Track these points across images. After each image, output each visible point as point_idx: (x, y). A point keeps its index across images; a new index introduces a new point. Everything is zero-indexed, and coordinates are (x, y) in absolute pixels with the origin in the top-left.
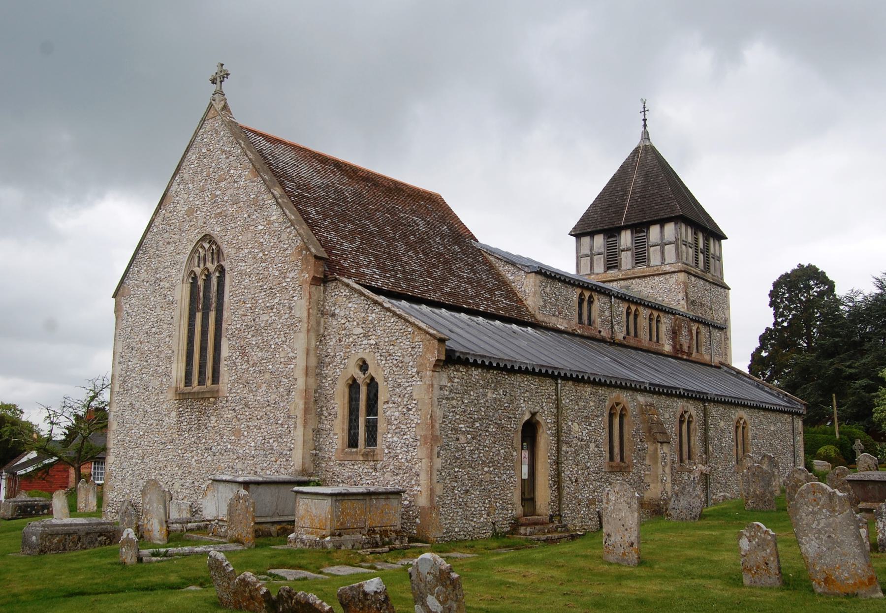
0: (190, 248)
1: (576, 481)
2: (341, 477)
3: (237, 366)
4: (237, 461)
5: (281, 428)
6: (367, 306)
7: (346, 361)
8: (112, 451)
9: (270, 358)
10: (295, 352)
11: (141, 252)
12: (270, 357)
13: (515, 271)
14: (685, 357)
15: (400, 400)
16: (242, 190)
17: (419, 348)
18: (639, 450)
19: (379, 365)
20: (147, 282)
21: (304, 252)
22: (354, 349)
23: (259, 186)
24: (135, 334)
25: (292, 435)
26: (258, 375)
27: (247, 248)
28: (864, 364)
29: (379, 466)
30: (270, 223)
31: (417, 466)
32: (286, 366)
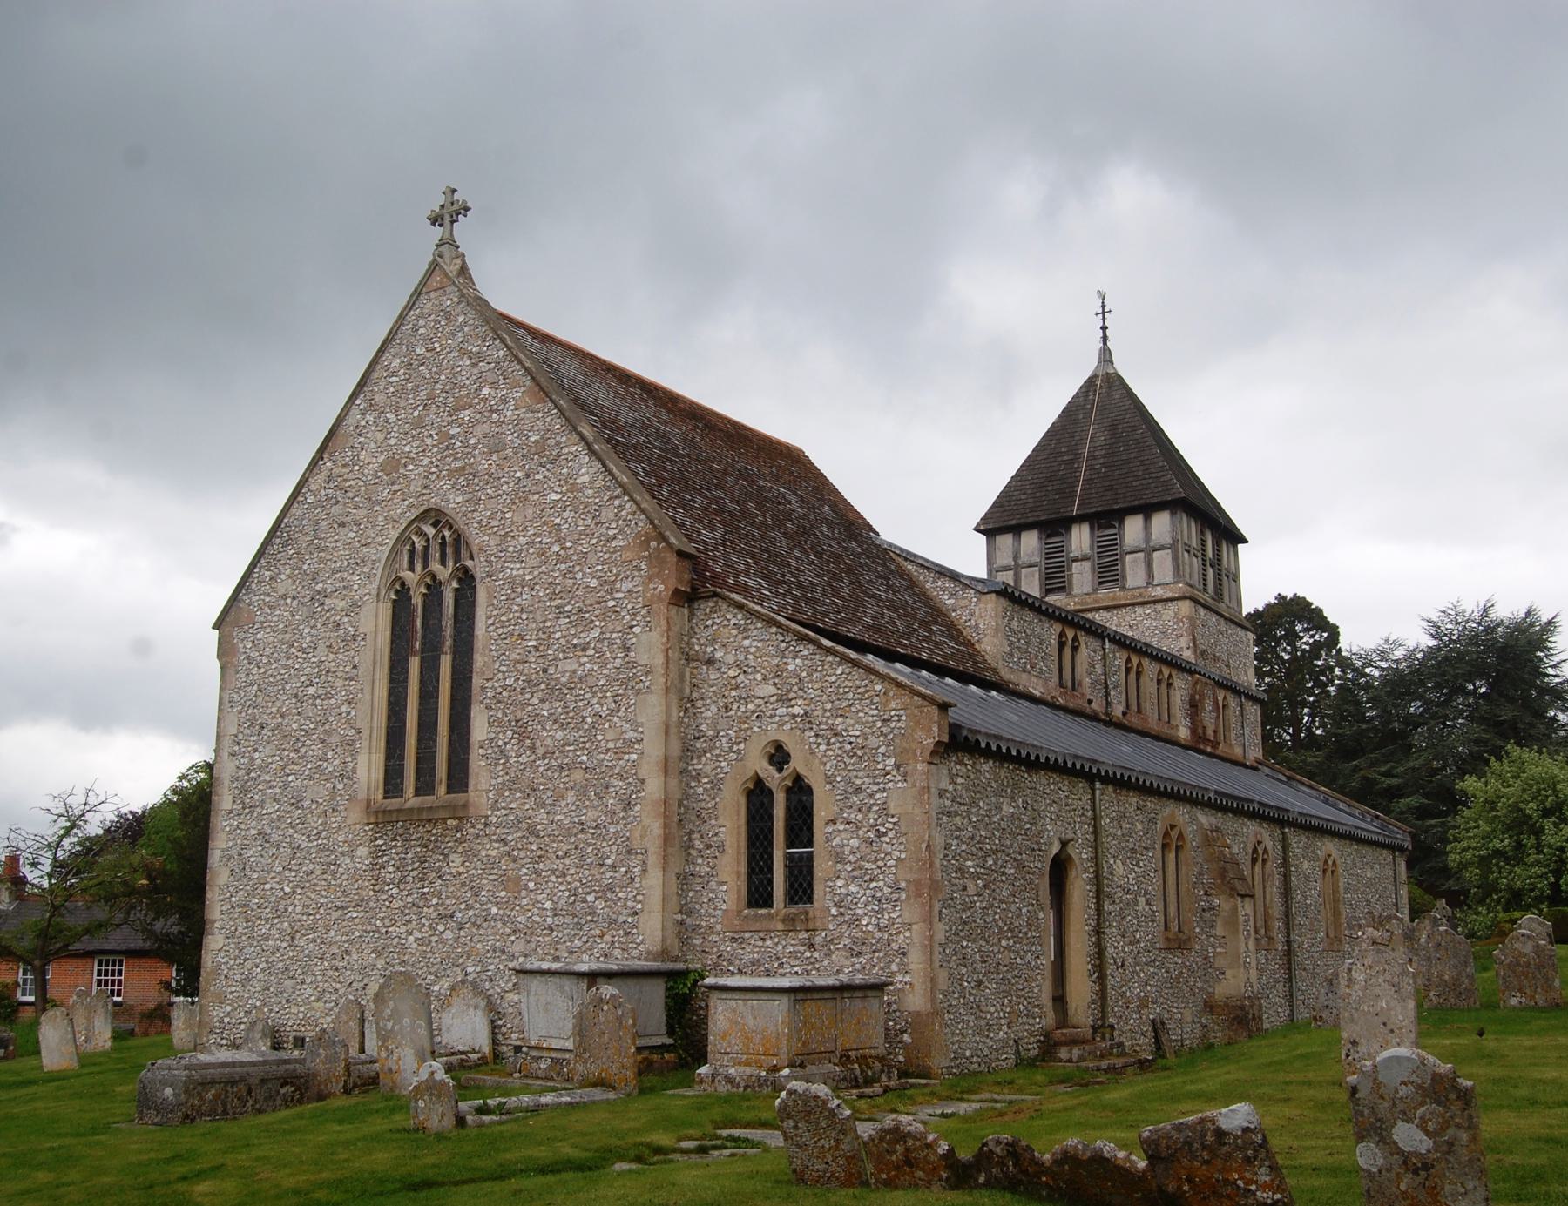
1: (1123, 965)
2: (737, 962)
3: (507, 758)
4: (513, 938)
5: (612, 874)
6: (784, 645)
7: (742, 746)
8: (217, 925)
9: (584, 742)
10: (640, 729)
11: (278, 541)
12: (582, 740)
13: (957, 589)
14: (1209, 749)
15: (860, 817)
16: (510, 427)
17: (899, 721)
18: (1204, 910)
19: (812, 753)
20: (294, 598)
21: (653, 544)
22: (759, 724)
23: (548, 419)
24: (267, 698)
25: (637, 885)
26: (556, 775)
27: (524, 536)
28: (1413, 769)
29: (818, 940)
30: (574, 488)
31: (902, 936)
32: (621, 755)
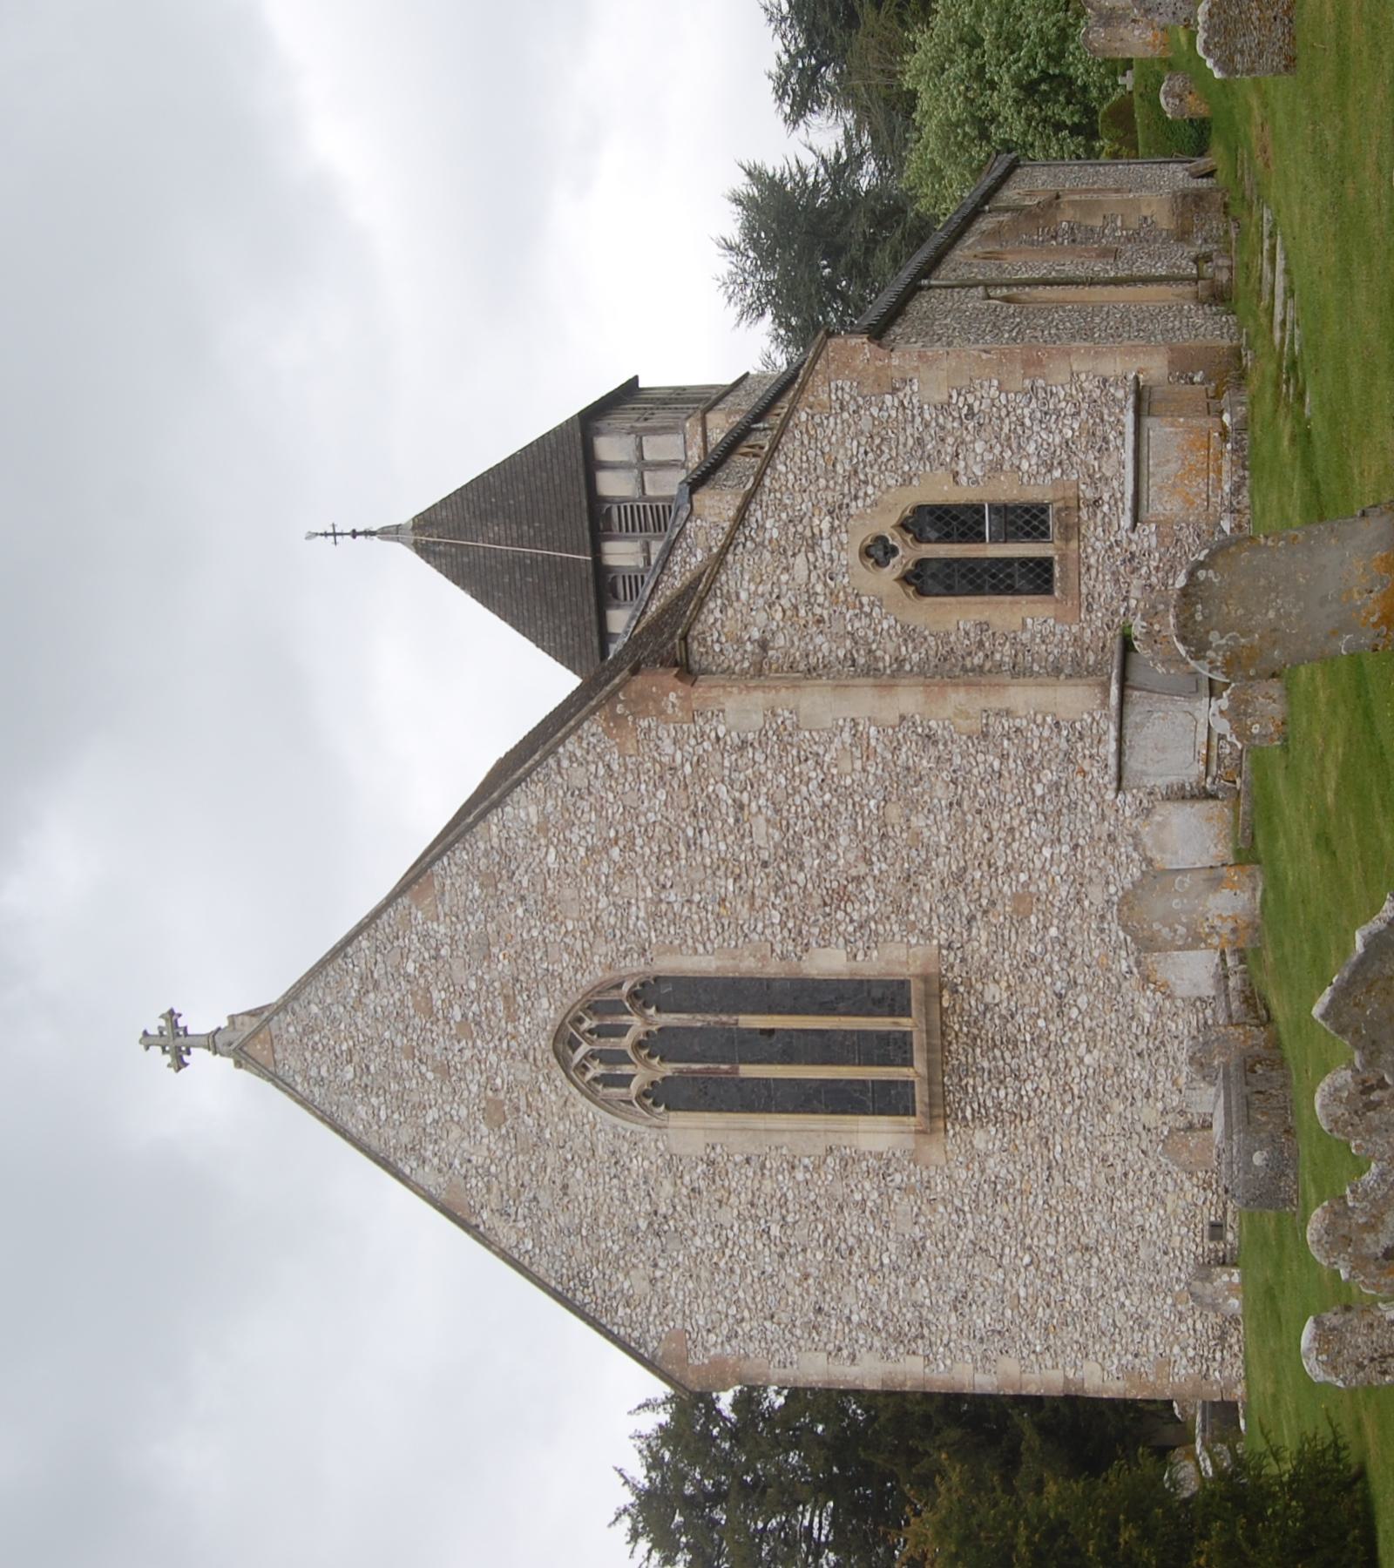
0: (583, 1104)
2: (1115, 603)
3: (870, 918)
4: (1086, 903)
5: (1011, 760)
6: (749, 544)
7: (865, 600)
8: (1071, 1375)
9: (854, 805)
10: (841, 722)
11: (579, 1295)
12: (850, 807)
13: (684, 545)
15: (950, 440)
17: (842, 389)
19: (875, 503)
20: (656, 1265)
21: (620, 709)
22: (840, 577)
24: (783, 1303)
25: (1025, 722)
26: (891, 844)
27: (598, 901)
29: (1089, 494)
30: (543, 828)
31: (1085, 385)
32: (871, 750)
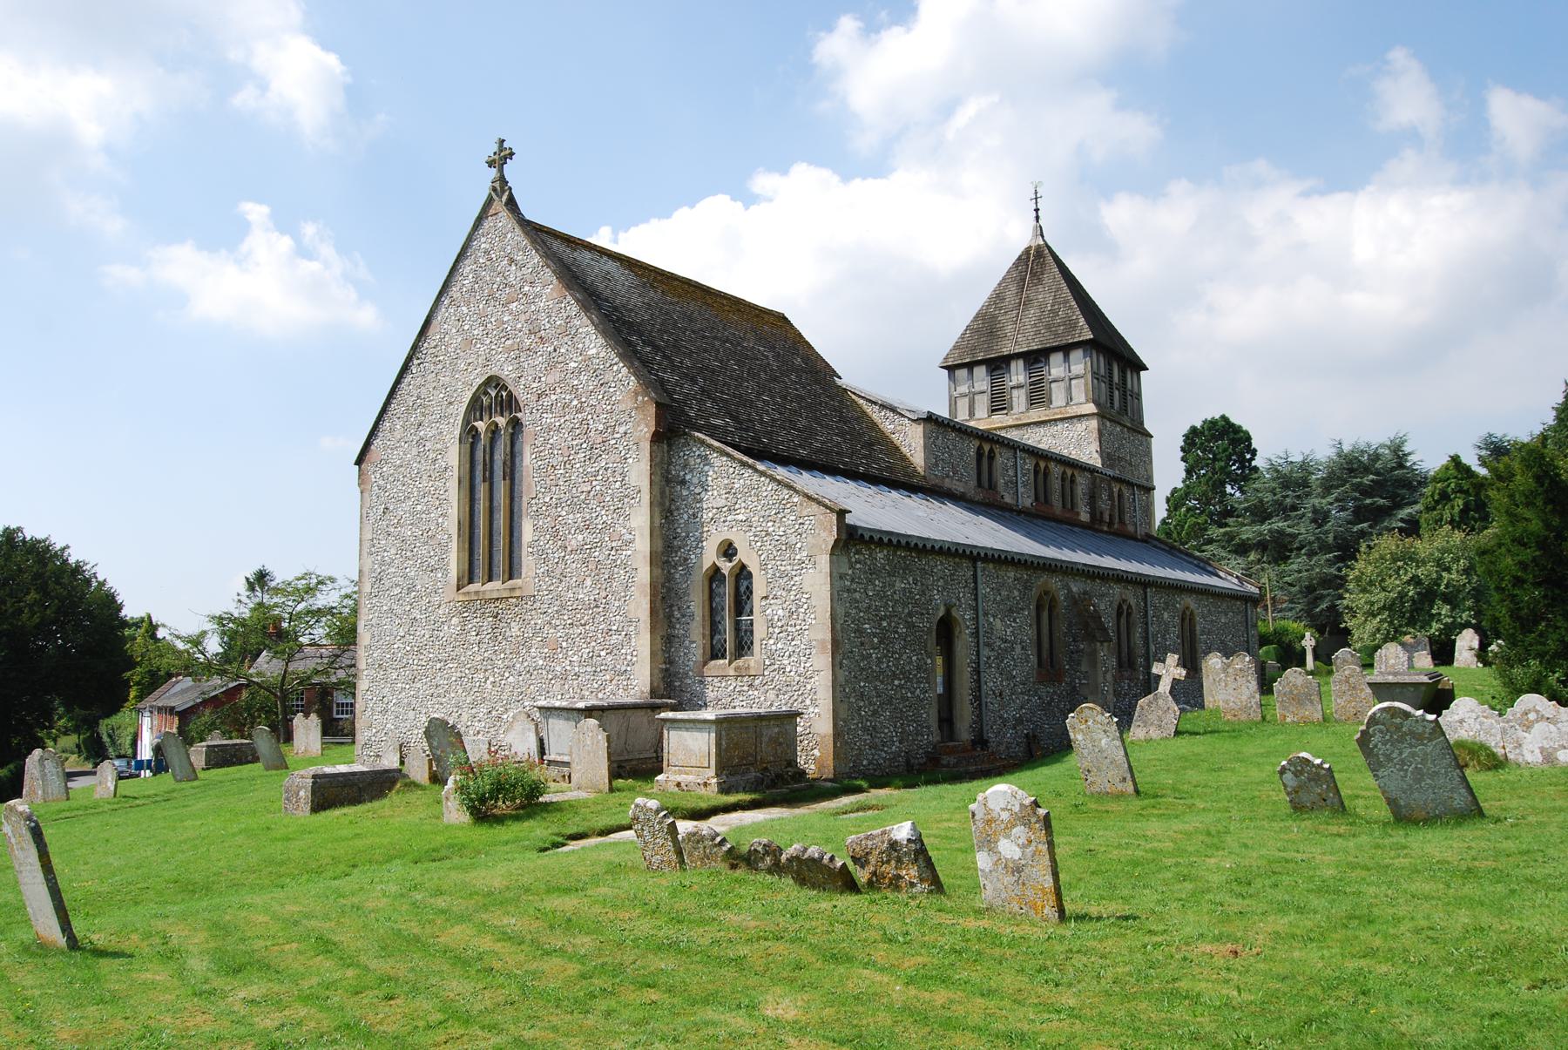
1: (1001, 695)
14: (1105, 528)
